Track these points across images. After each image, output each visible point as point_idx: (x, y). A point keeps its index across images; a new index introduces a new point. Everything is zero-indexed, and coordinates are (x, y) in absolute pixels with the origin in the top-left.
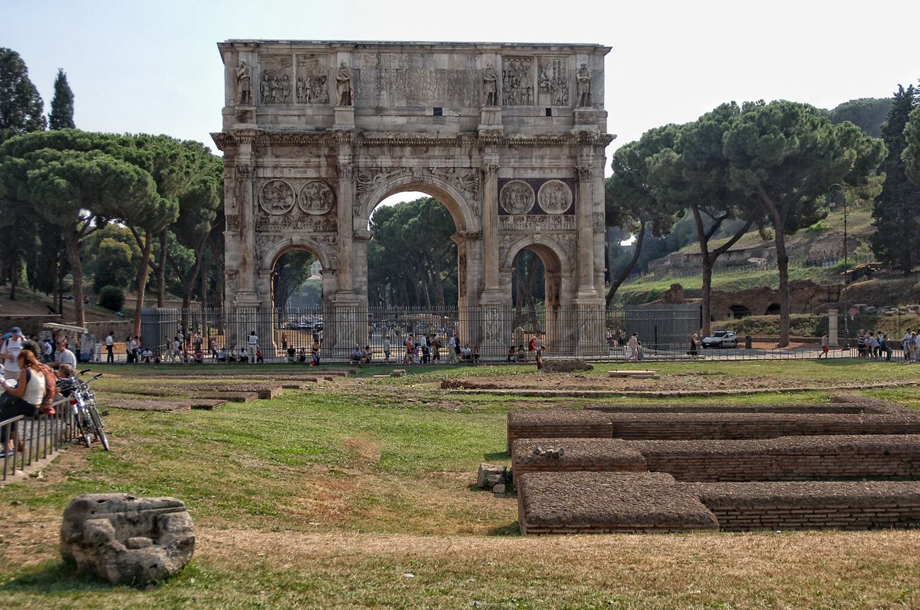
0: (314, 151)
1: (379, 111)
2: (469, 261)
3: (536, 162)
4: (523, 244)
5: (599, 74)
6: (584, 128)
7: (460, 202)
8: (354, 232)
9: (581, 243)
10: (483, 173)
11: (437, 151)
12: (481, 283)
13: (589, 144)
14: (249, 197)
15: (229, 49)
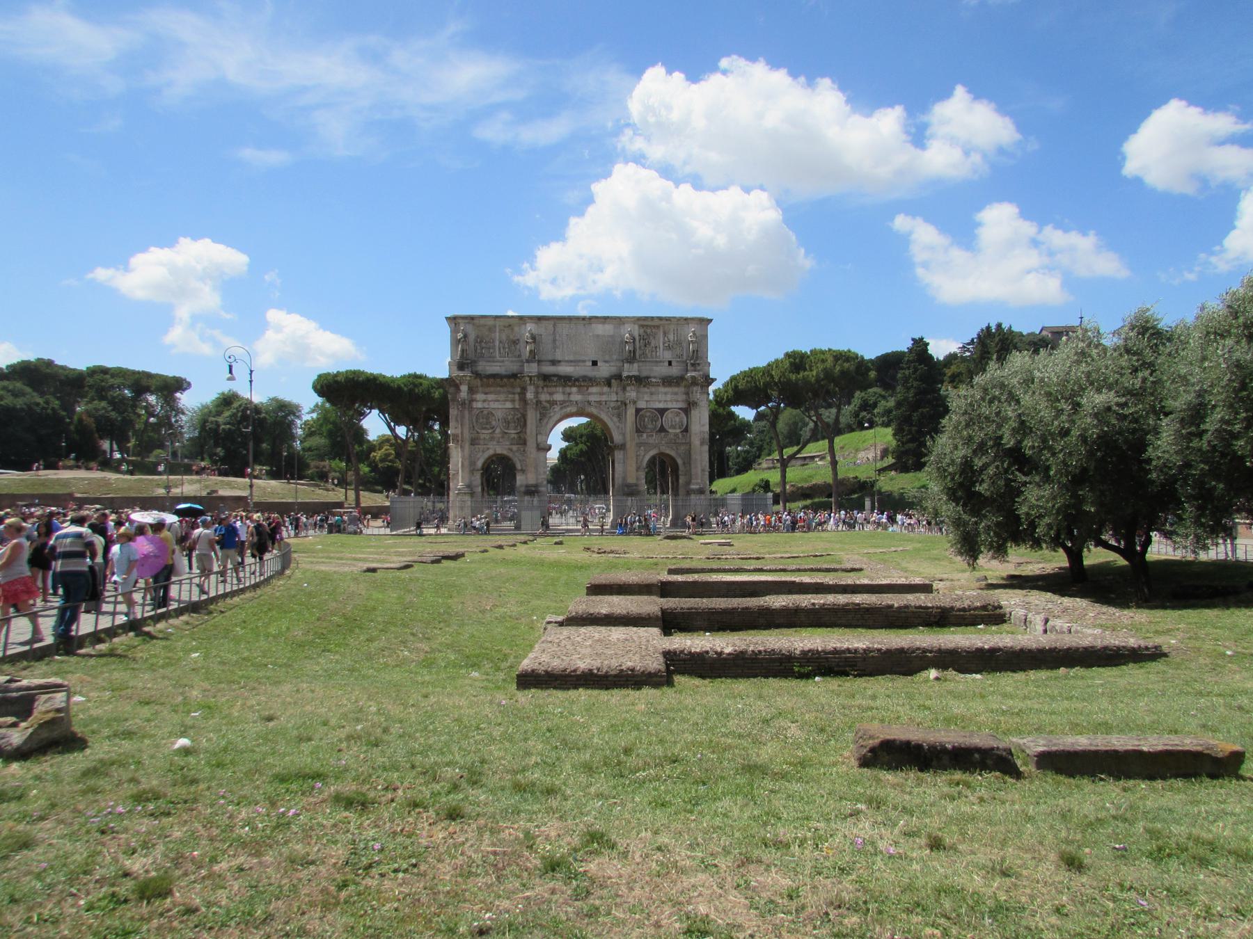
0: (510, 390)
1: (554, 362)
2: (616, 465)
3: (661, 397)
4: (653, 453)
5: (706, 336)
6: (693, 374)
7: (610, 424)
8: (538, 445)
9: (692, 452)
10: (626, 405)
11: (594, 390)
12: (624, 479)
13: (697, 385)
14: (467, 421)
15: (454, 320)
